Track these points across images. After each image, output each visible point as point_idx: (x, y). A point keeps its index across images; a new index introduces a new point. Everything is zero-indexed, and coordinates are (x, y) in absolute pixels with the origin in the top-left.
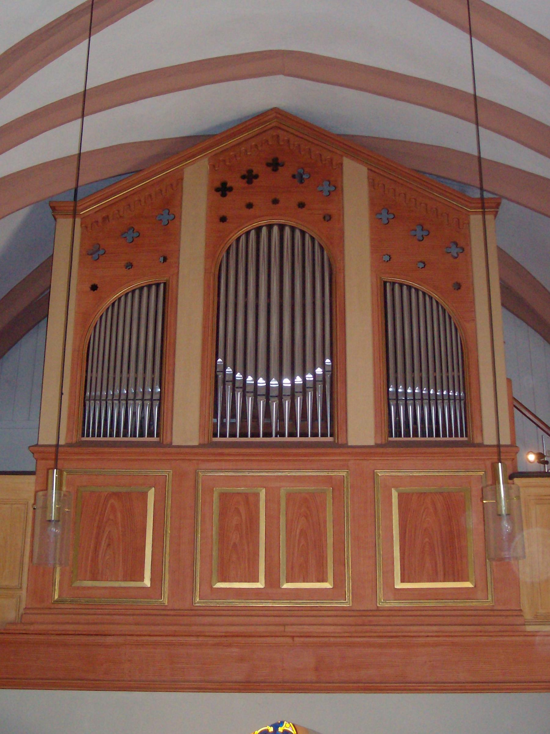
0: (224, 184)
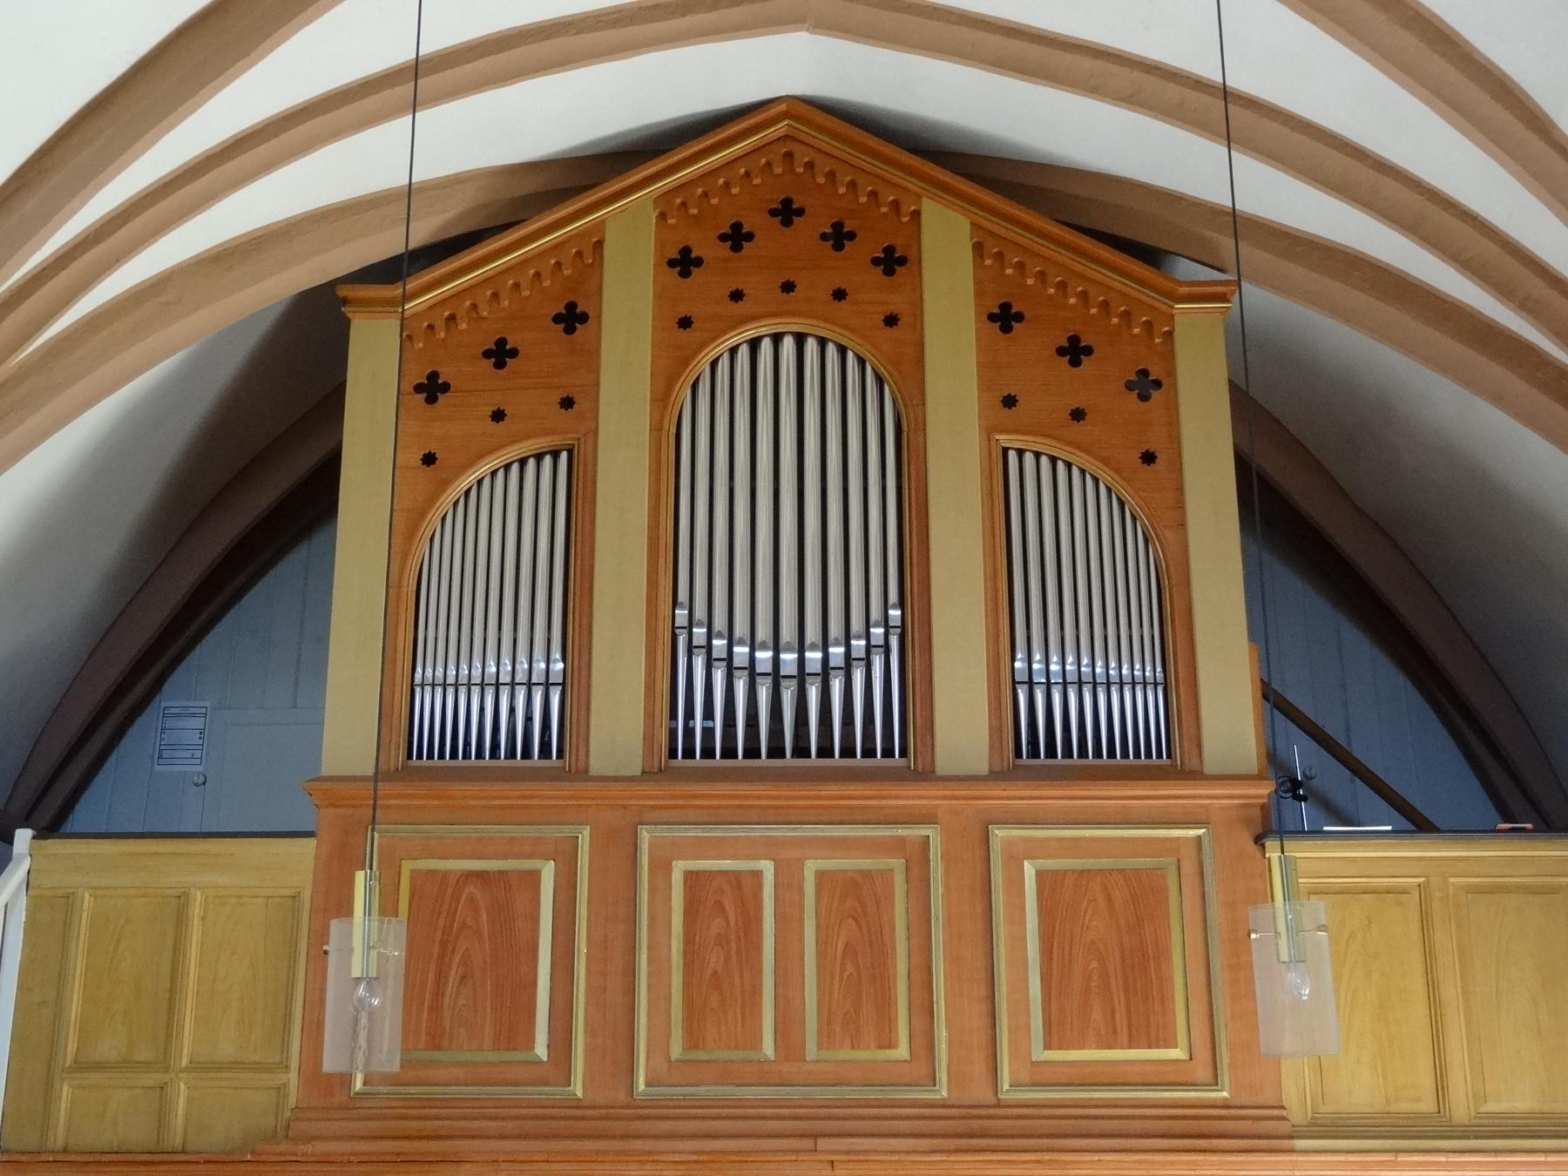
0: (686, 251)
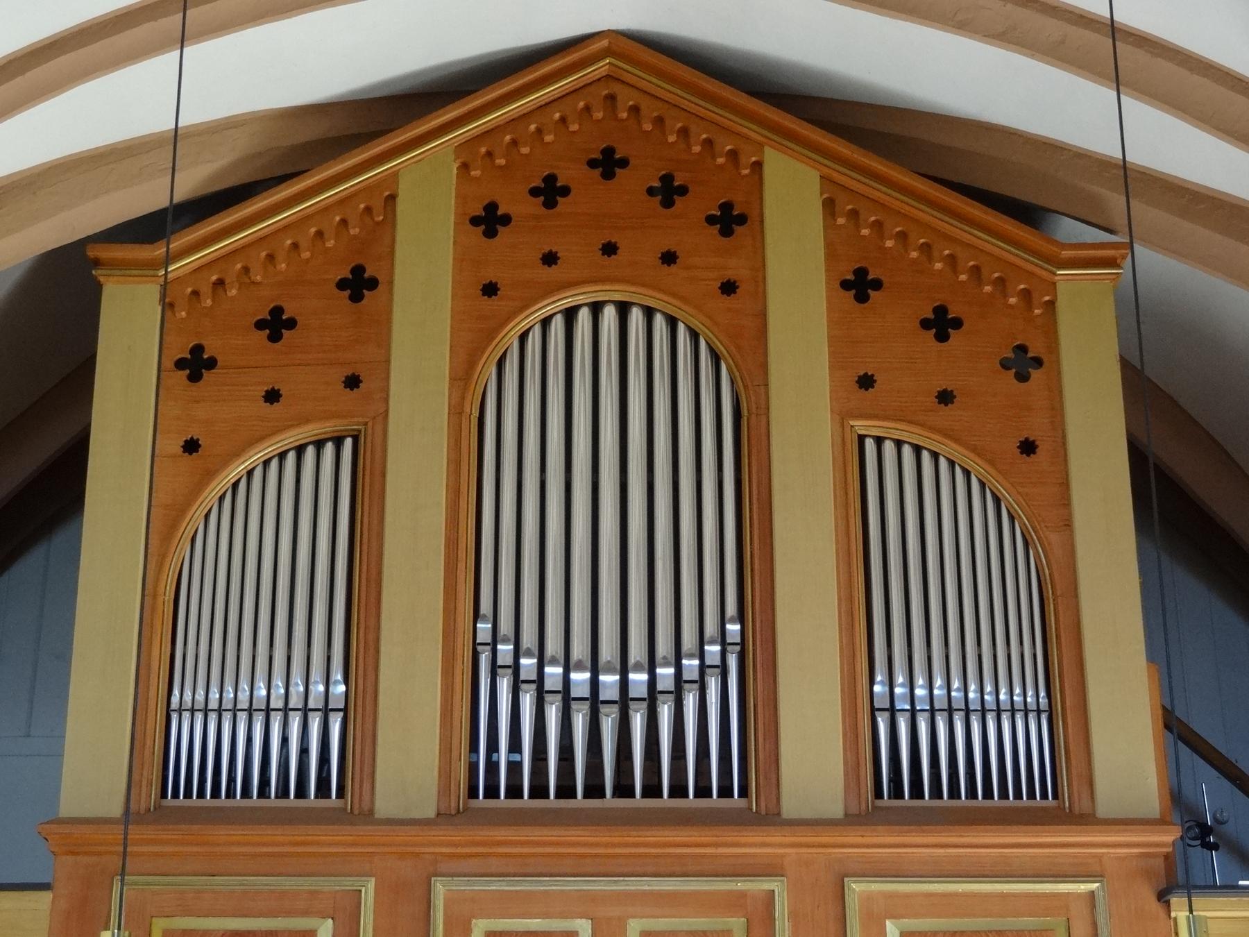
0: (491, 207)
